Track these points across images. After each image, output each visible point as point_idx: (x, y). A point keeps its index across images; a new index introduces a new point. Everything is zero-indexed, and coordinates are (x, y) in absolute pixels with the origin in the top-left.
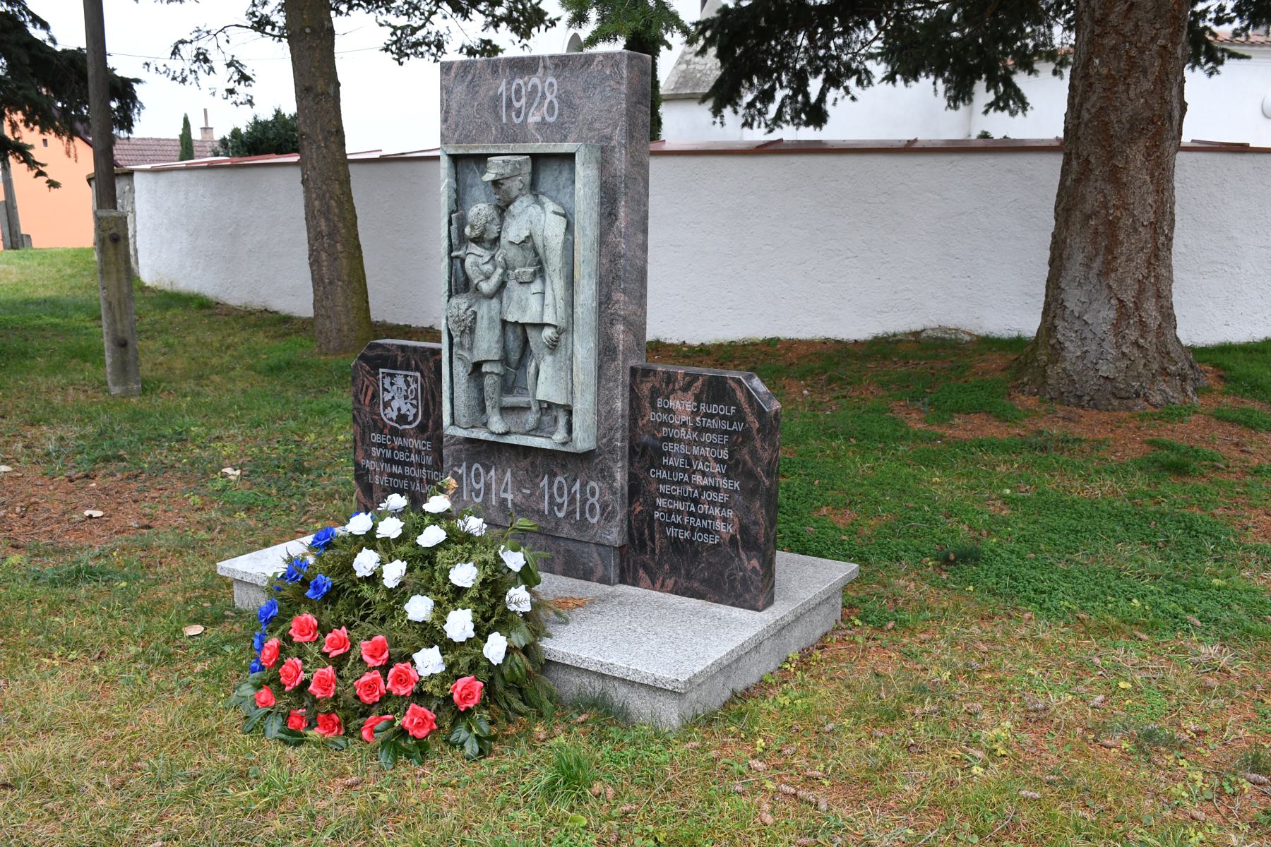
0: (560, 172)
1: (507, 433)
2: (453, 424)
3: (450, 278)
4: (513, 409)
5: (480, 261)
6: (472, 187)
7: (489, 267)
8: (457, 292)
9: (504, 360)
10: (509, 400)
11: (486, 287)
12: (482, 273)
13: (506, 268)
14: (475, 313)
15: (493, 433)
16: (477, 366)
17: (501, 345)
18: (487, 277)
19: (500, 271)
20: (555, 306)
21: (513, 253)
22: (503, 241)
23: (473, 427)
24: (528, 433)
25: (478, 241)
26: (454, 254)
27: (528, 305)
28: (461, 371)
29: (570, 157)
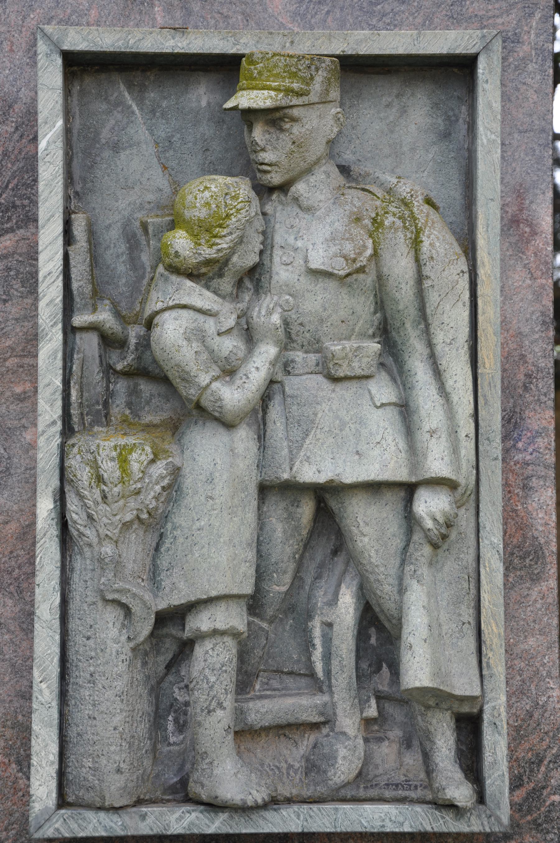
0: (403, 111)
1: (274, 802)
2: (63, 802)
3: (66, 382)
4: (286, 729)
5: (210, 325)
6: (116, 148)
7: (229, 345)
8: (87, 429)
9: (254, 604)
10: (265, 709)
11: (232, 396)
12: (214, 357)
13: (288, 339)
14: (176, 472)
15: (214, 806)
16: (171, 618)
17: (251, 555)
18: (229, 371)
19: (267, 352)
20: (453, 432)
21: (318, 300)
22: (282, 273)
23: (139, 802)
24: (337, 796)
25: (202, 273)
26: (78, 320)
27: (350, 440)
28: (110, 643)
29: (458, 70)
